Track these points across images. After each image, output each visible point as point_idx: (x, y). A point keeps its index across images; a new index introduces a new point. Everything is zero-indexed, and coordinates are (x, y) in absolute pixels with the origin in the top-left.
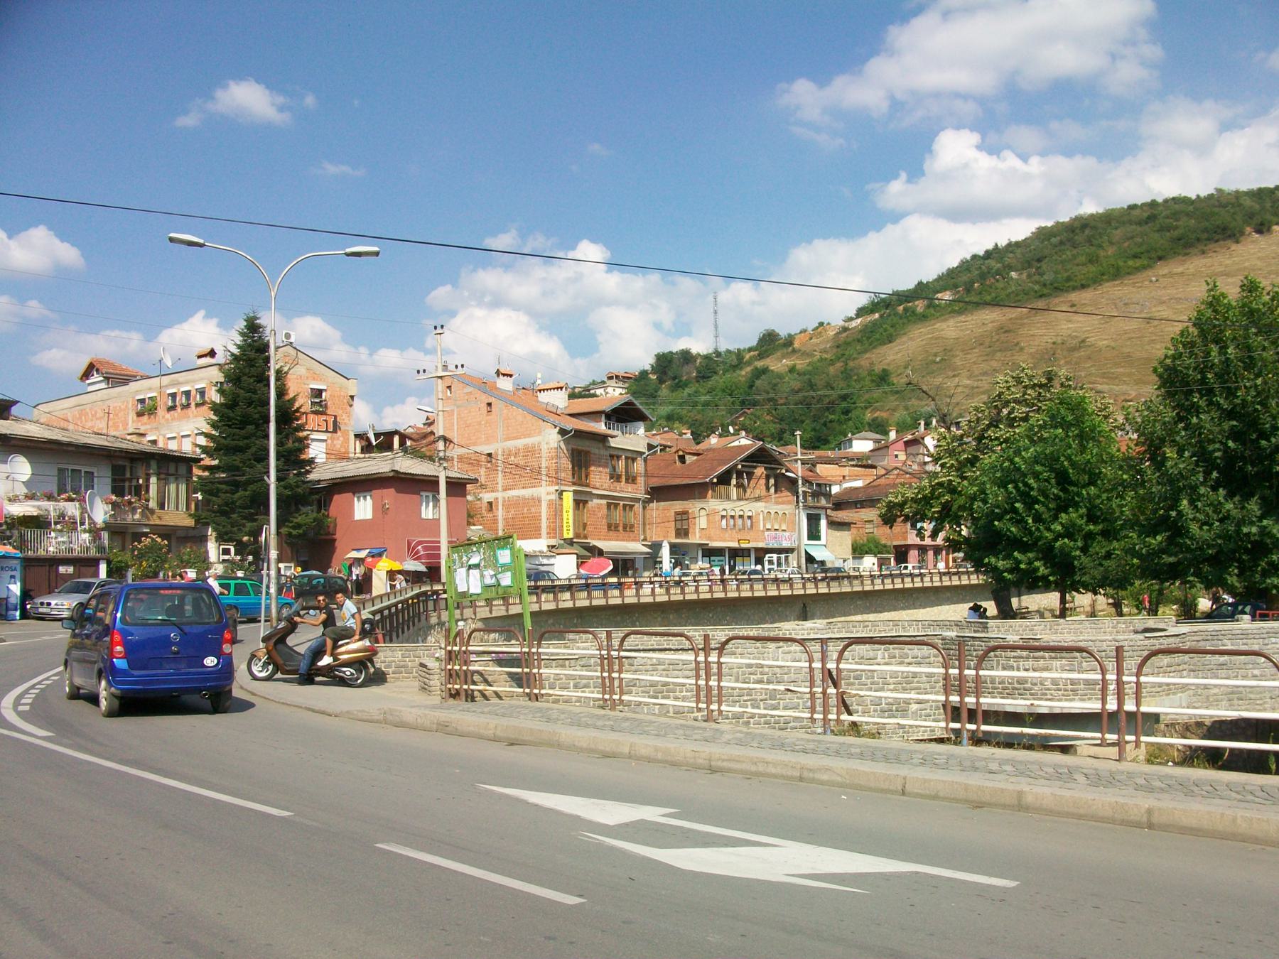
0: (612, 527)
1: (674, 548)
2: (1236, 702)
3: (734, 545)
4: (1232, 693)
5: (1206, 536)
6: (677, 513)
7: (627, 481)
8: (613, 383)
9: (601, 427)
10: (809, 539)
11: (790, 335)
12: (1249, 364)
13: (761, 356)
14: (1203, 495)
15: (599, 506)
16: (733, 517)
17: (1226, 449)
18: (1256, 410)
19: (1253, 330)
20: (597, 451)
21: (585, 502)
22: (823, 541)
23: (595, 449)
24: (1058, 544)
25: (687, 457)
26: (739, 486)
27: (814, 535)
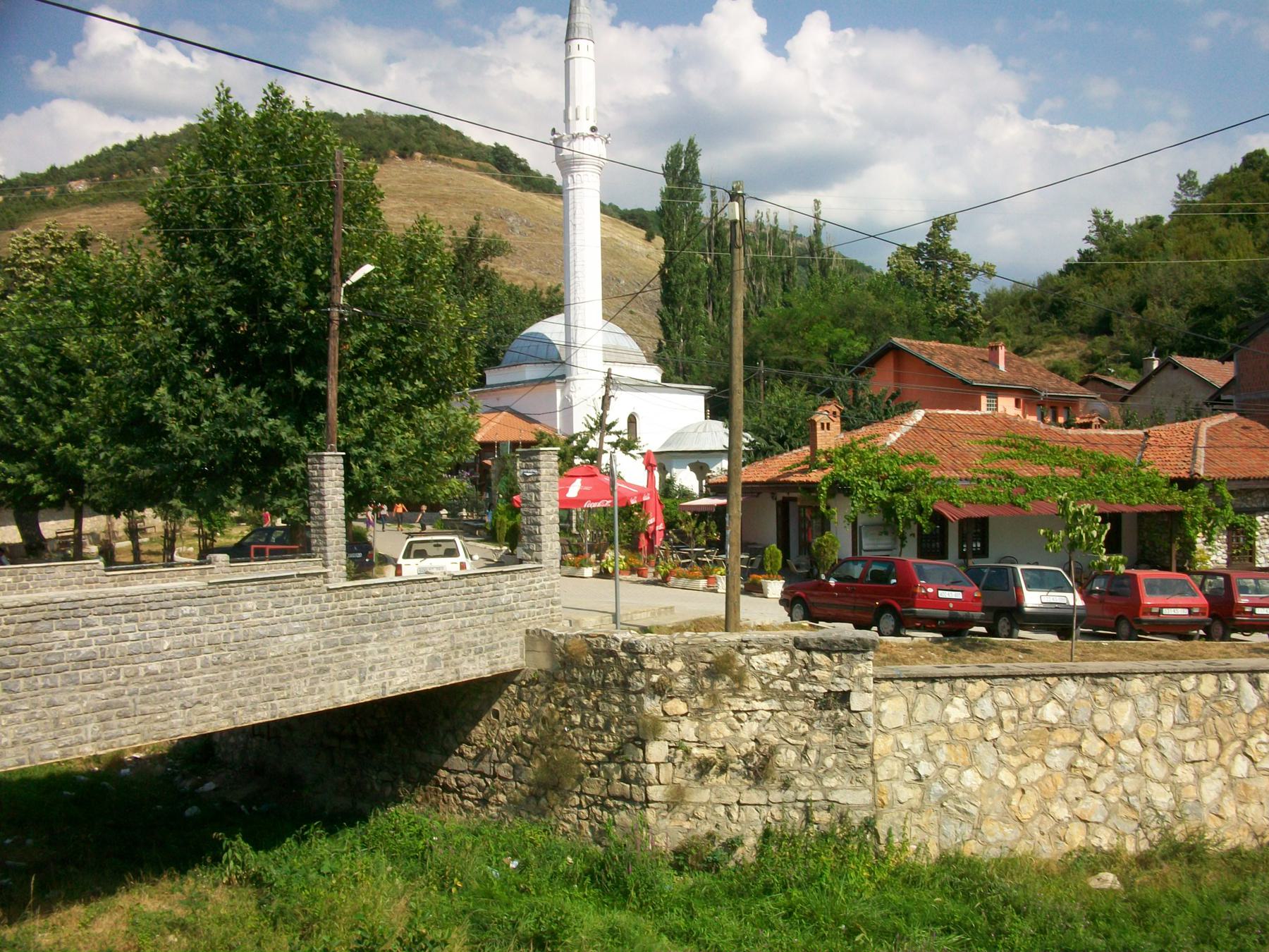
2: (115, 722)
4: (108, 707)
5: (192, 439)
12: (265, 202)
14: (192, 382)
17: (226, 322)
18: (264, 266)
19: (276, 155)
24: (57, 451)
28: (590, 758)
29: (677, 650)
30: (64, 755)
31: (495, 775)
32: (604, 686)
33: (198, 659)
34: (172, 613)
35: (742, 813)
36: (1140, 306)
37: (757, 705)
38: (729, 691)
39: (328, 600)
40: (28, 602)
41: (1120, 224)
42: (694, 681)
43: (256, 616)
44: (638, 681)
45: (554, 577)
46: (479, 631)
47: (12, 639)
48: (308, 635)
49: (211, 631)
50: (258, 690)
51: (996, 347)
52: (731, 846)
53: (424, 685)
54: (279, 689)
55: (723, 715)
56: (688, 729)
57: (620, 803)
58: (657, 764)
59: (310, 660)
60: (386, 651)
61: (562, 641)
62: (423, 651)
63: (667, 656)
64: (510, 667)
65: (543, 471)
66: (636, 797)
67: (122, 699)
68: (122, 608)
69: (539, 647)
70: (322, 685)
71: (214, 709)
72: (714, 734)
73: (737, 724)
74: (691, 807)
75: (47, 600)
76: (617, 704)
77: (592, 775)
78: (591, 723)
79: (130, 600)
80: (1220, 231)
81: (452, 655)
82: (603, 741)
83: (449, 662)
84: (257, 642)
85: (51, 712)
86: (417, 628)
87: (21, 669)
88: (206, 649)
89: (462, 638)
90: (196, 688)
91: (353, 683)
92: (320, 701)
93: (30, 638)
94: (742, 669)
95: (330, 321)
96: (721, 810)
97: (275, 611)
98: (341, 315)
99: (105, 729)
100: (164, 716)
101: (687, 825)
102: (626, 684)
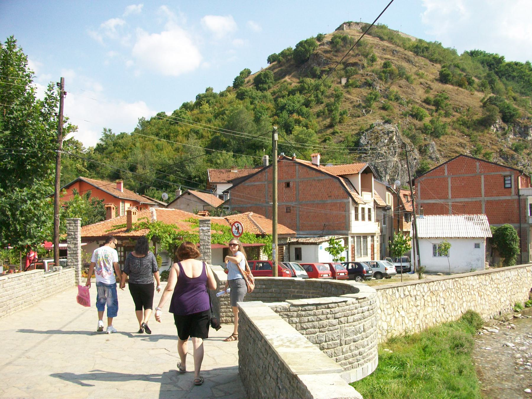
36: (133, 169)
41: (114, 134)
51: (120, 183)
80: (157, 142)
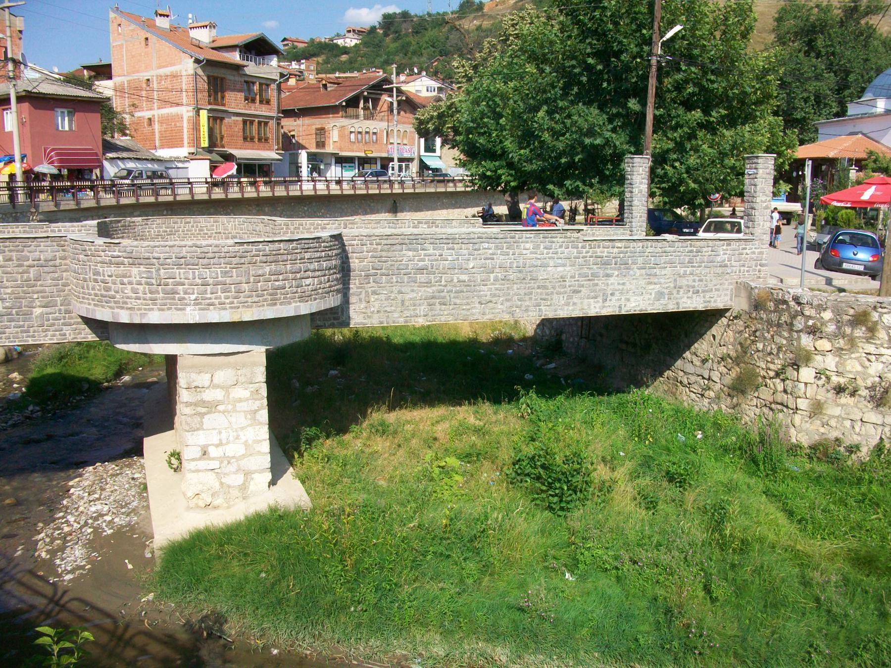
0: (247, 139)
1: (312, 157)
3: (362, 155)
4: (433, 297)
6: (317, 129)
7: (261, 102)
8: (351, 35)
9: (235, 57)
10: (426, 151)
11: (481, 2)
13: (459, 18)
15: (235, 122)
16: (360, 133)
20: (232, 78)
21: (222, 119)
22: (438, 153)
23: (230, 76)
25: (328, 85)
26: (366, 108)
27: (430, 148)
28: (765, 374)
29: (829, 304)
30: (406, 322)
31: (709, 379)
32: (779, 325)
33: (492, 276)
34: (476, 246)
35: (863, 429)
37: (883, 351)
38: (863, 338)
39: (583, 247)
40: (389, 234)
42: (839, 328)
43: (531, 253)
44: (799, 323)
45: (764, 247)
46: (697, 278)
47: (379, 254)
48: (568, 268)
49: (500, 259)
50: (531, 299)
52: (853, 449)
53: (650, 310)
54: (544, 300)
55: (857, 355)
56: (830, 362)
57: (779, 407)
58: (806, 384)
59: (568, 284)
60: (624, 284)
61: (756, 291)
62: (652, 287)
63: (821, 308)
64: (721, 306)
65: (760, 171)
66: (790, 405)
67: (442, 294)
68: (445, 241)
69: (743, 294)
70: (575, 300)
71: (500, 307)
72: (848, 368)
73: (867, 363)
74: (826, 418)
75: (400, 233)
76: (785, 338)
77: (766, 386)
78: (769, 348)
79: (449, 237)
81: (675, 292)
82: (774, 363)
83: (672, 297)
84: (531, 269)
85: (400, 297)
86: (649, 271)
87: (383, 271)
88: (497, 270)
89: (683, 282)
90: (489, 293)
91: (598, 302)
92: (573, 310)
93: (390, 254)
94: (876, 323)
95: (650, 66)
96: (848, 424)
97: (545, 251)
98: (658, 62)
99: (431, 310)
100: (468, 307)
101: (822, 430)
102: (792, 324)
